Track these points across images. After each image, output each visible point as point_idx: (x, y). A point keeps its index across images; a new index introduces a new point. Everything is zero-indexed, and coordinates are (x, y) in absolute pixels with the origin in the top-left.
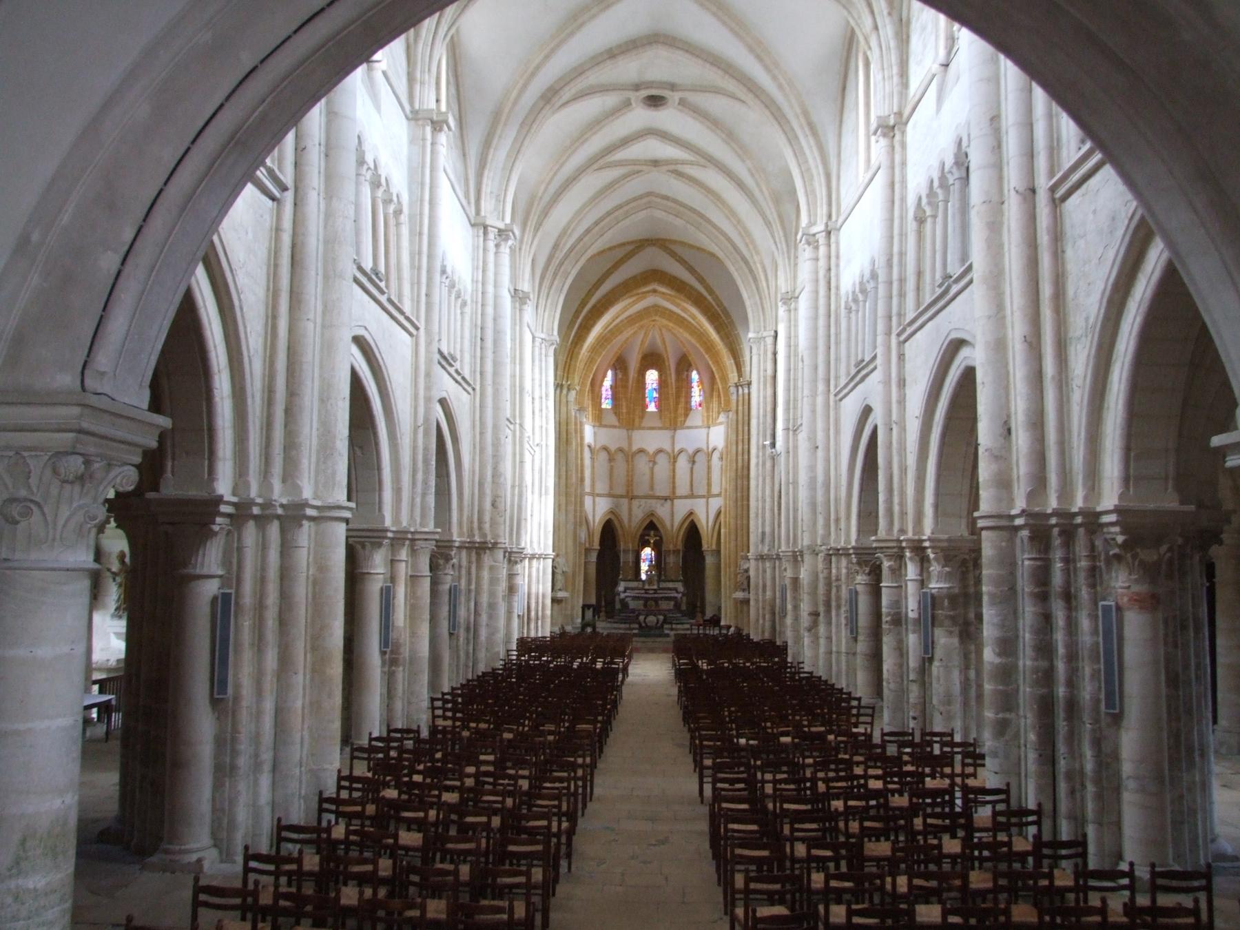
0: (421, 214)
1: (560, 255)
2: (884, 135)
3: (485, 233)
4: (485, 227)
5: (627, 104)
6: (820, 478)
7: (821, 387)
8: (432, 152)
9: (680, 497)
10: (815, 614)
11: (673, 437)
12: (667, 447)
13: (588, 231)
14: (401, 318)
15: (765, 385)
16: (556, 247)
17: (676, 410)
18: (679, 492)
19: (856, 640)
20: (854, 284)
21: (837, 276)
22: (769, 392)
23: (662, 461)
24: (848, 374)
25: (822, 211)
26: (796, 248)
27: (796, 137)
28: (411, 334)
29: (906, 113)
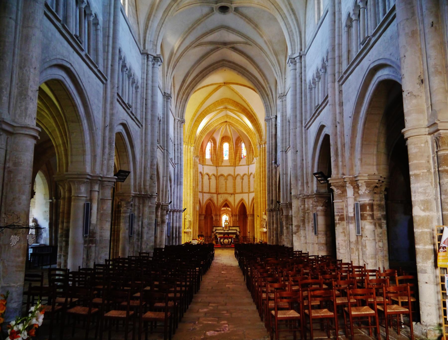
12: (232, 173)
15: (272, 138)
18: (237, 191)
21: (305, 76)
25: (298, 48)
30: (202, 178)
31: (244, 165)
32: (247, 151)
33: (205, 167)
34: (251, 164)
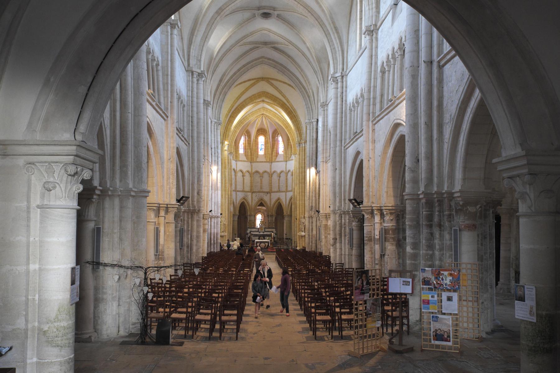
0: (167, 66)
1: (223, 84)
2: (368, 35)
3: (192, 75)
4: (192, 72)
5: (254, 16)
6: (337, 182)
7: (338, 143)
8: (171, 39)
9: (274, 192)
10: (335, 239)
11: (271, 166)
12: (269, 171)
13: (235, 74)
14: (161, 112)
16: (221, 81)
17: (272, 154)
18: (273, 190)
19: (352, 249)
20: (353, 99)
22: (314, 146)
23: (266, 176)
24: (350, 138)
25: (340, 67)
26: (327, 83)
27: (329, 34)
28: (164, 119)
29: (378, 25)
30: (235, 175)
31: (281, 161)
32: (284, 146)
33: (239, 163)
34: (289, 160)
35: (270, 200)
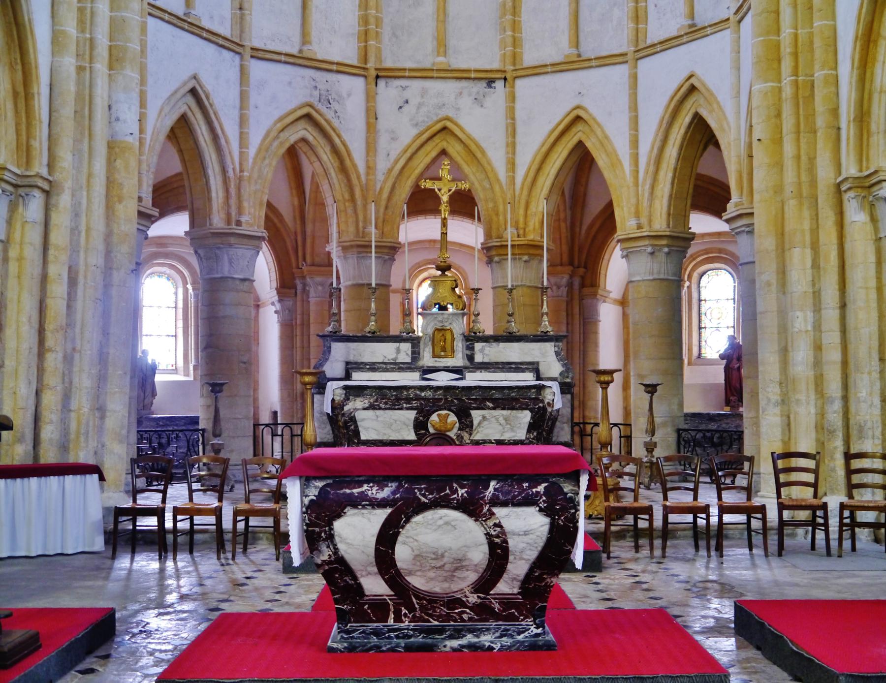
9: (538, 71)
35: (512, 131)
